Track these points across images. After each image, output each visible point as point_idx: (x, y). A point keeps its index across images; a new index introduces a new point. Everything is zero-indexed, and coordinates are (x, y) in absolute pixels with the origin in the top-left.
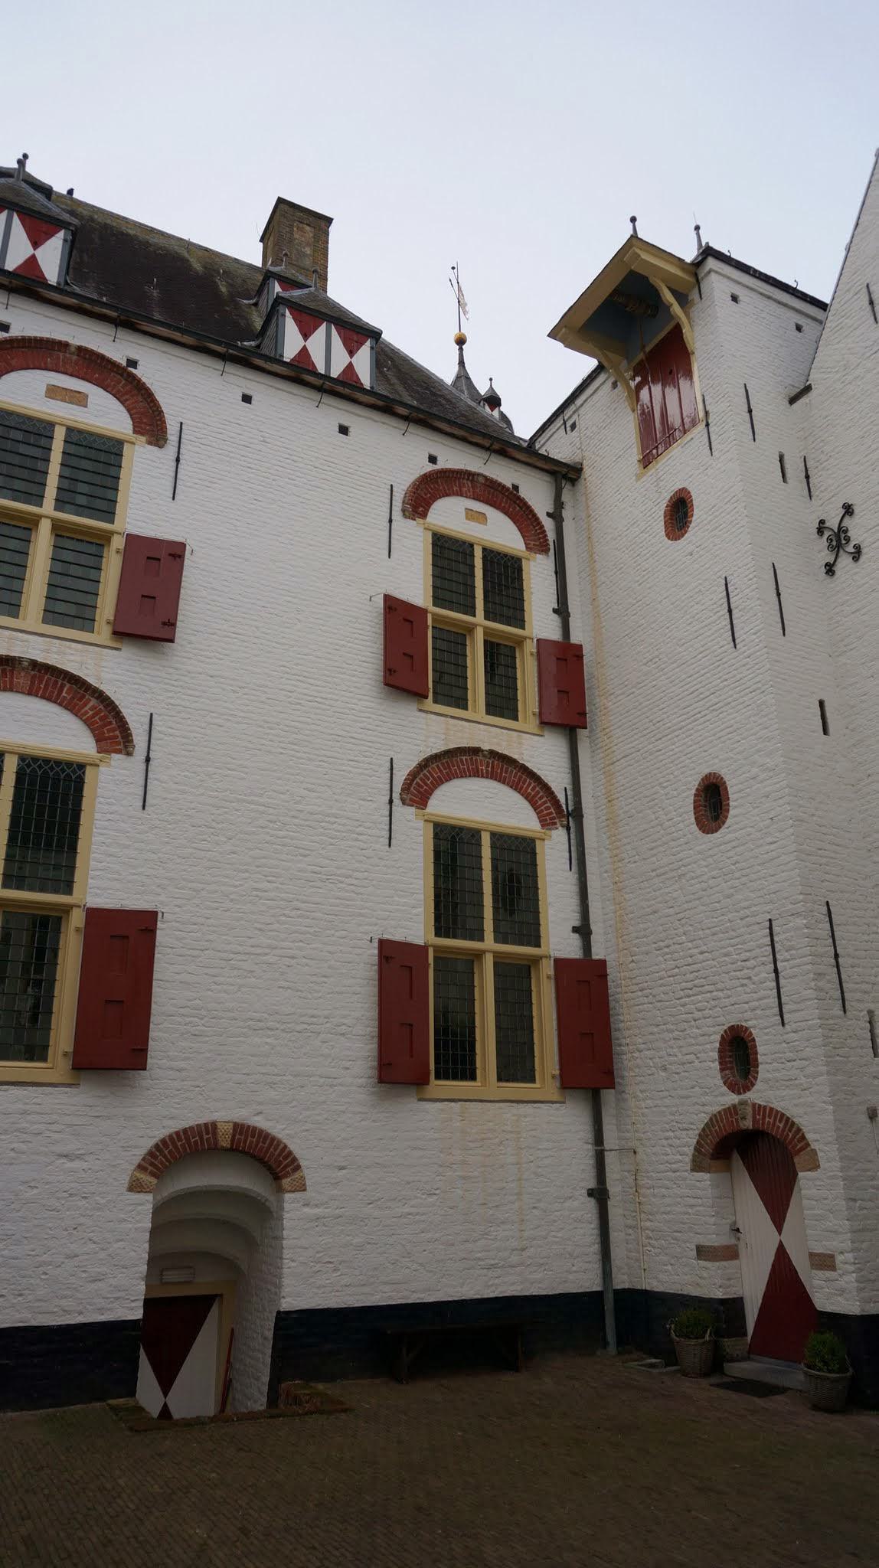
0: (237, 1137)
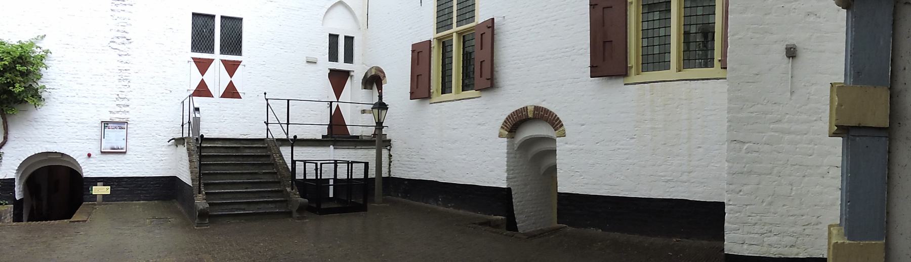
0: (536, 112)
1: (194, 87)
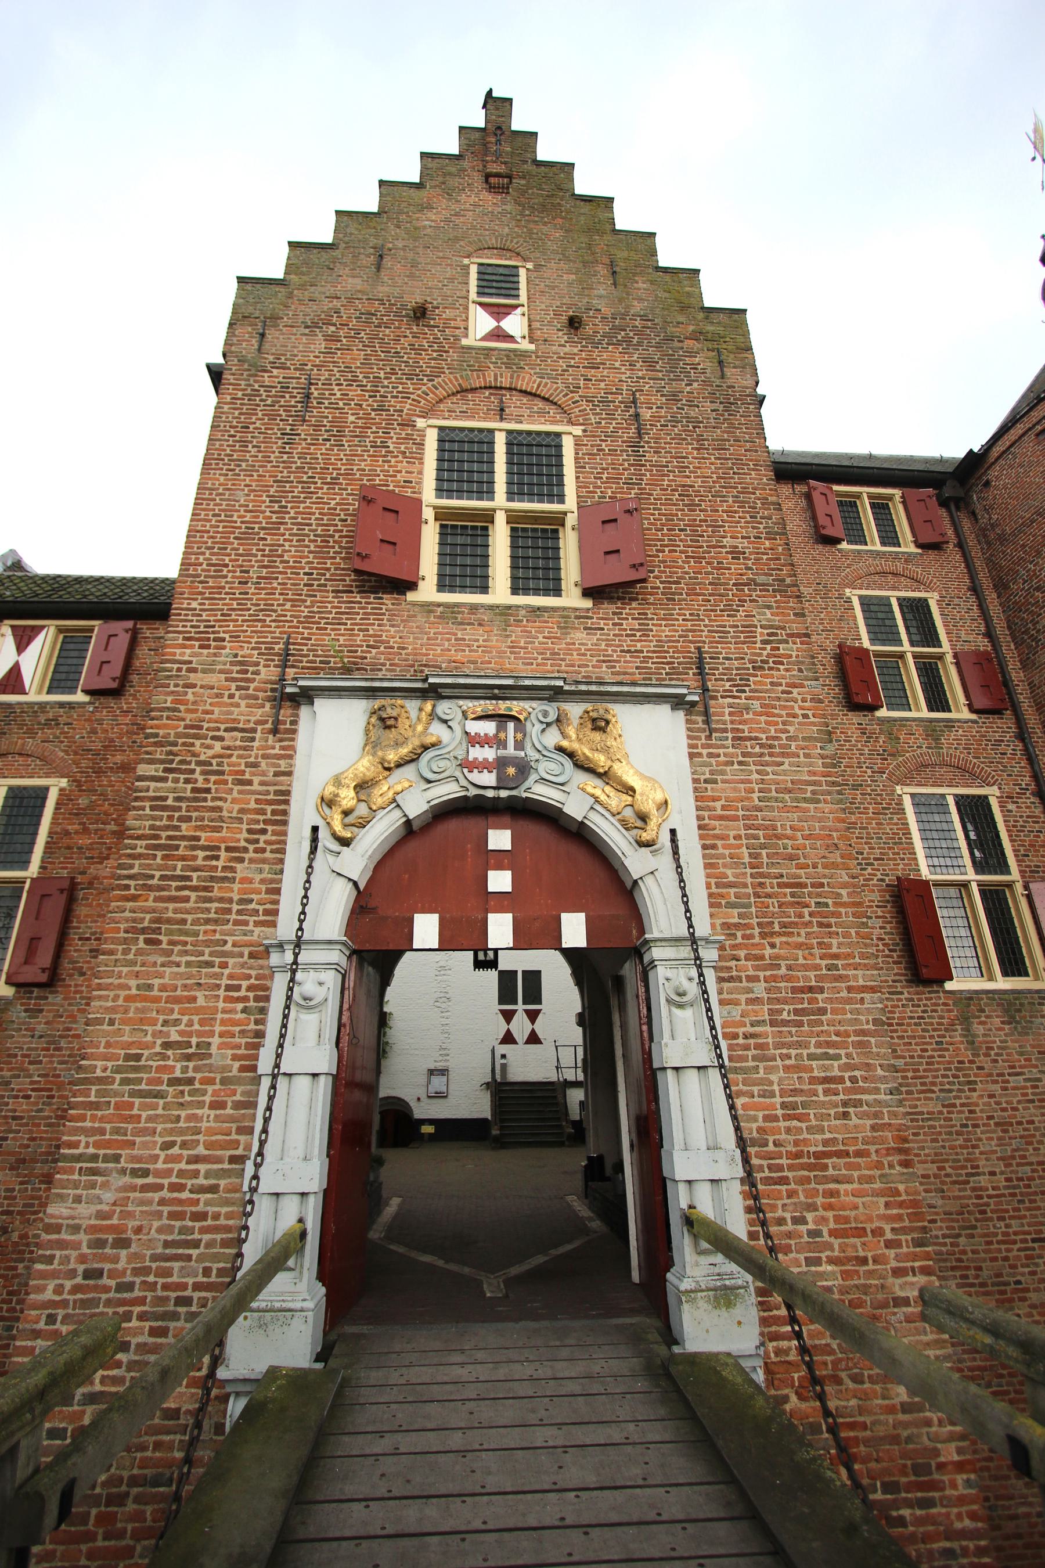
1: (501, 1036)
